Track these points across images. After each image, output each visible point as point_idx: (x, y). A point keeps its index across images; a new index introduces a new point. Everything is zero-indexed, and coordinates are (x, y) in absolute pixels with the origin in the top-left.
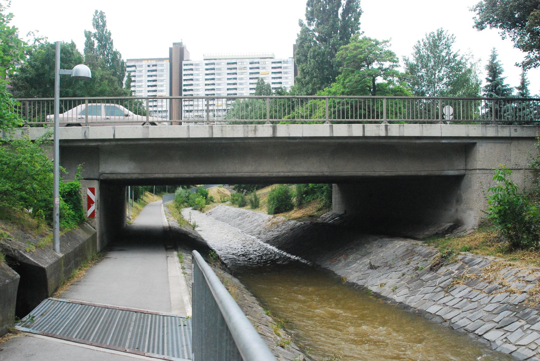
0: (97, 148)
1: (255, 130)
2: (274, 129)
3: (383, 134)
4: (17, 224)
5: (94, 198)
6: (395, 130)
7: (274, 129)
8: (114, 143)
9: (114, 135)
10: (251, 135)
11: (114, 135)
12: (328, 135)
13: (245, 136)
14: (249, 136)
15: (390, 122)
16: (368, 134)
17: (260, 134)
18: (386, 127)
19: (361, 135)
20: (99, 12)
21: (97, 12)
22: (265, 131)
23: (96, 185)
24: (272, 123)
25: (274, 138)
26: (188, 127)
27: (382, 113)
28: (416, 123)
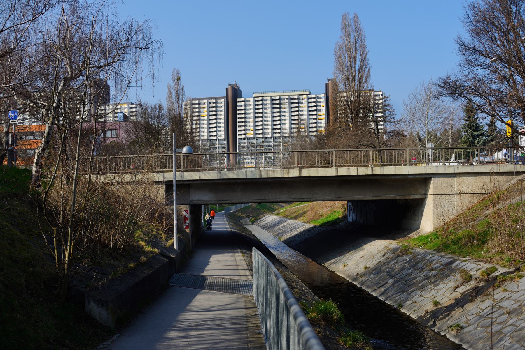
0: (189, 185)
1: (288, 173)
2: (300, 172)
3: (370, 173)
4: (138, 229)
5: (188, 216)
6: (379, 171)
7: (300, 172)
8: (199, 182)
9: (200, 177)
10: (286, 176)
11: (200, 177)
12: (335, 175)
13: (282, 176)
14: (285, 176)
15: (374, 165)
16: (360, 174)
17: (291, 175)
18: (372, 168)
19: (356, 174)
20: (176, 69)
21: (174, 69)
22: (294, 173)
23: (187, 208)
24: (299, 167)
25: (300, 177)
26: (246, 171)
27: (370, 160)
28: (391, 165)
